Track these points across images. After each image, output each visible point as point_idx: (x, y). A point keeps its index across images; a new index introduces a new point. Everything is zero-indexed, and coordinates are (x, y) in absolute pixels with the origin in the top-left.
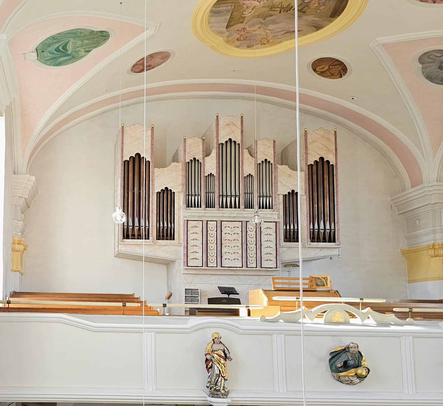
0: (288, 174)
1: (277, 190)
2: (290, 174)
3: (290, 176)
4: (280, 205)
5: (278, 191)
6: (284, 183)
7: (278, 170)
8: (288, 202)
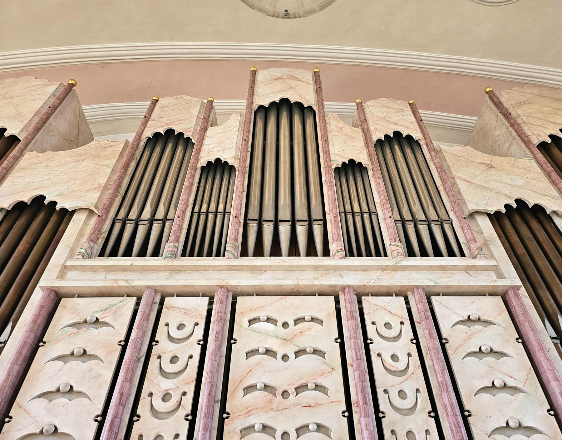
0: (482, 163)
1: (459, 202)
2: (489, 162)
3: (490, 167)
4: (491, 246)
5: (465, 203)
6: (475, 181)
7: (445, 154)
8: (515, 239)
